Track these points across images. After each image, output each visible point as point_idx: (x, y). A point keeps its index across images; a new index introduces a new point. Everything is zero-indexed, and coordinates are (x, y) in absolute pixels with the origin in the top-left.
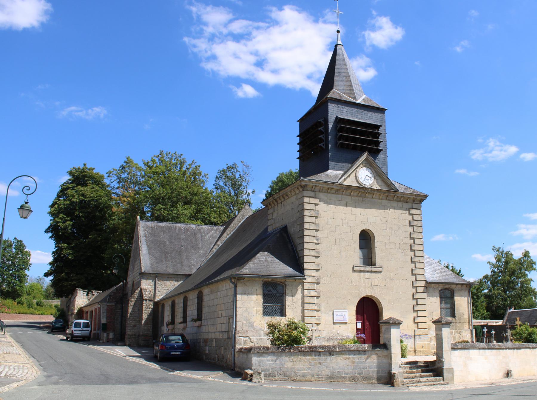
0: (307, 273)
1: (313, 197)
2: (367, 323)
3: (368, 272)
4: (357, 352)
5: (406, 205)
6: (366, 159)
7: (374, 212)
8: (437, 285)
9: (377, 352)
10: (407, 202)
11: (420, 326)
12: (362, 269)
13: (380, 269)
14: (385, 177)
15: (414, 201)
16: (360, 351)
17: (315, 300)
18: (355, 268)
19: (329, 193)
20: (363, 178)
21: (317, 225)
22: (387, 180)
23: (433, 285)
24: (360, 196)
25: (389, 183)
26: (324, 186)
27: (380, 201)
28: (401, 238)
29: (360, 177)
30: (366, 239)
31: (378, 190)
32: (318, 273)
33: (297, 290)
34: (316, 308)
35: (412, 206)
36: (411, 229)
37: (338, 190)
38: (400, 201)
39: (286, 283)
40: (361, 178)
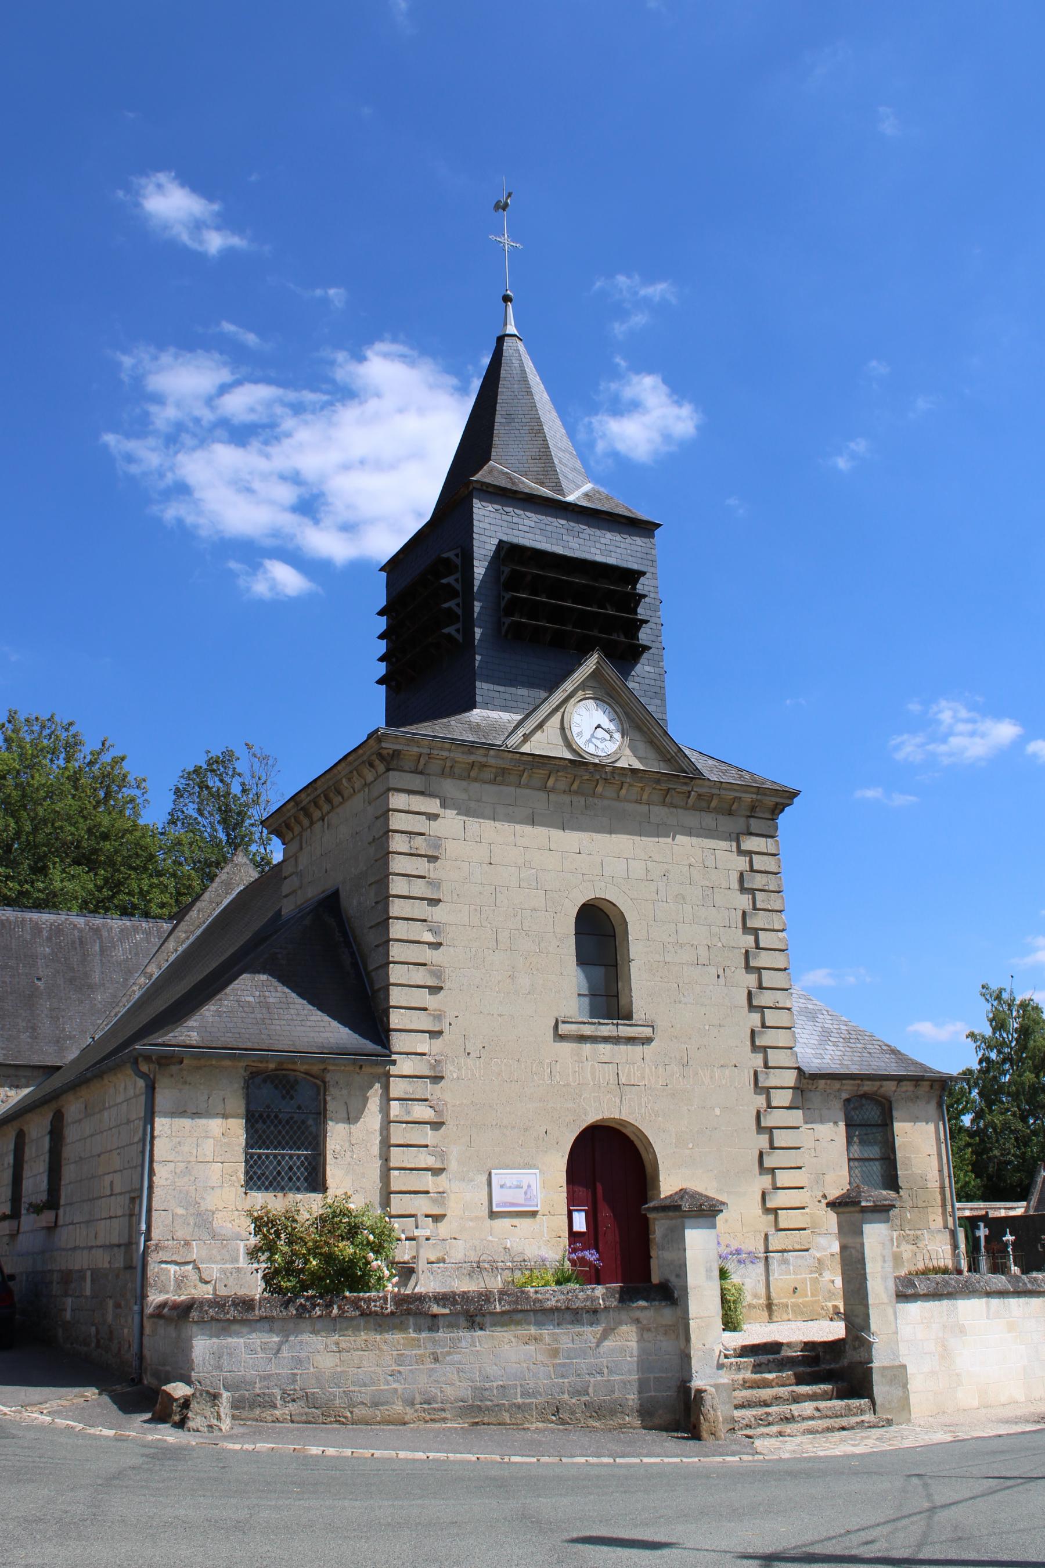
0: (399, 1042)
1: (422, 793)
2: (605, 1213)
3: (606, 1040)
4: (568, 1316)
5: (726, 823)
6: (595, 675)
7: (622, 843)
8: (837, 1085)
9: (638, 1314)
10: (730, 813)
11: (786, 1219)
12: (587, 1030)
13: (647, 1032)
14: (657, 732)
15: (752, 812)
16: (576, 1312)
17: (429, 1136)
18: (563, 1029)
19: (476, 780)
20: (587, 735)
21: (435, 884)
22: (665, 742)
23: (822, 1083)
24: (576, 793)
25: (673, 750)
26: (459, 756)
27: (644, 808)
28: (714, 929)
29: (575, 730)
30: (599, 933)
31: (634, 771)
32: (438, 1042)
33: (366, 1100)
34: (431, 1161)
35: (748, 826)
36: (744, 901)
37: (503, 771)
38: (708, 810)
39: (328, 1077)
40: (580, 734)
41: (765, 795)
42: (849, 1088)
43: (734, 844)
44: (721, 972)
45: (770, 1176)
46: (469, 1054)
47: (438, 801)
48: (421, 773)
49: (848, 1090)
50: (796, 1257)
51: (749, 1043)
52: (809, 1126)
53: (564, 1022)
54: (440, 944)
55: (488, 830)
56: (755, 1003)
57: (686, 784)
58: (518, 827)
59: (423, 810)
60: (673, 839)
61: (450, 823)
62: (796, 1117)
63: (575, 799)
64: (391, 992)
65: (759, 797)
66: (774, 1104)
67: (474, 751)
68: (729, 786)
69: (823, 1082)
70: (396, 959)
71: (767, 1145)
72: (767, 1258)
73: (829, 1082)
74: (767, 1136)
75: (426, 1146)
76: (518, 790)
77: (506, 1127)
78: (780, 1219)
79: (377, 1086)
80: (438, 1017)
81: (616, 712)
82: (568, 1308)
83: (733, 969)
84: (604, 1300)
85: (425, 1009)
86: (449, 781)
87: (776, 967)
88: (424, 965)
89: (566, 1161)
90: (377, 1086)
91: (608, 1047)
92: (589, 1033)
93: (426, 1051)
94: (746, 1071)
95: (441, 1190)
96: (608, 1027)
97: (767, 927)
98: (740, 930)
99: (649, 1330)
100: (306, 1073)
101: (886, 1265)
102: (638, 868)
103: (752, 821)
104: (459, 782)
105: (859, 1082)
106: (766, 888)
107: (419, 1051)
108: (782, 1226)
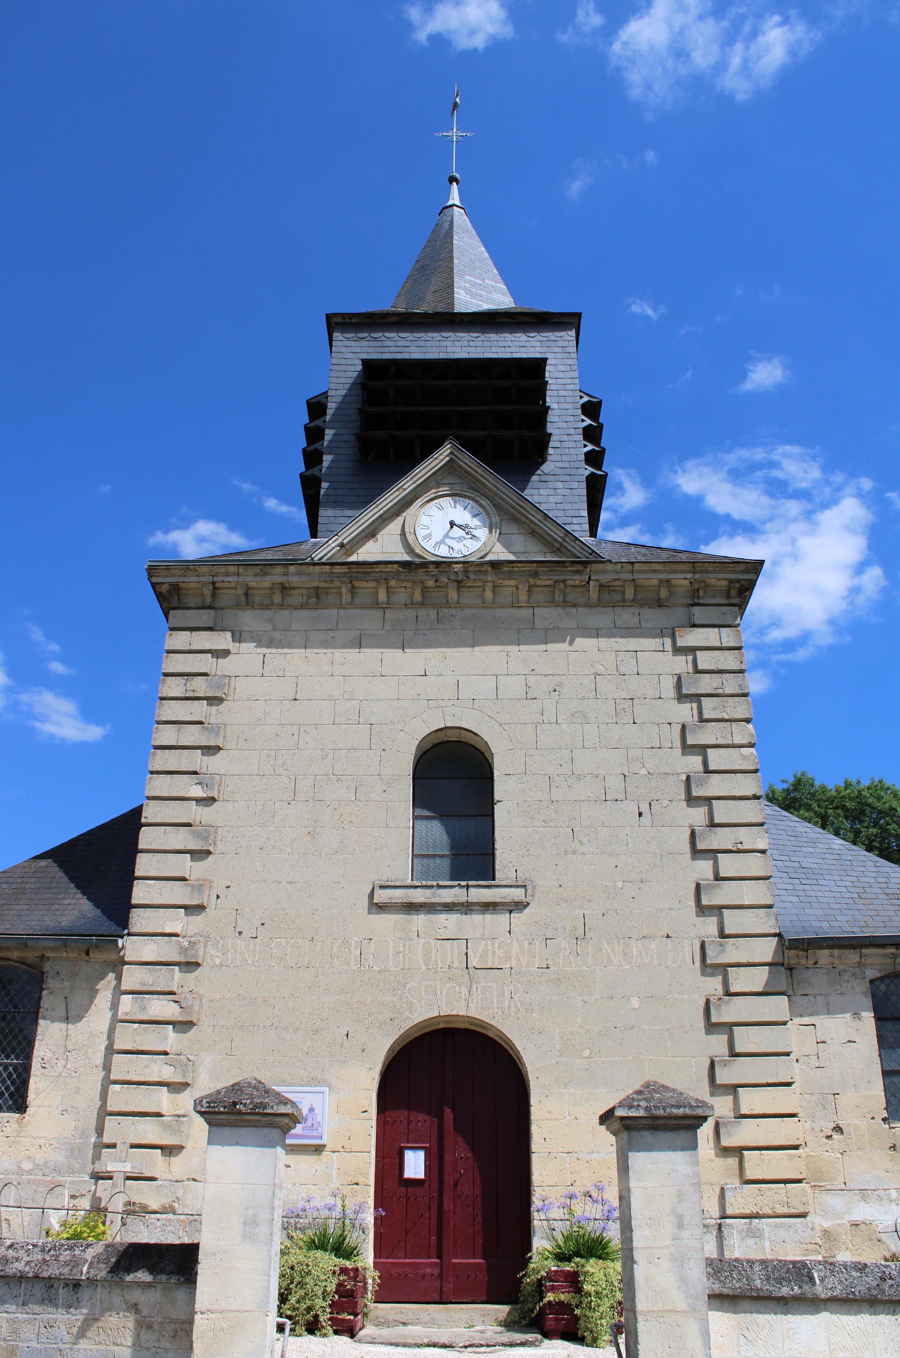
0: (139, 920)
1: (211, 629)
2: (459, 1151)
3: (450, 907)
4: (38, 1290)
5: (653, 617)
6: (450, 467)
7: (492, 656)
8: (852, 957)
9: (137, 1296)
10: (659, 604)
11: (757, 1165)
12: (419, 896)
13: (517, 894)
14: (535, 517)
15: (695, 597)
16: (50, 1283)
17: (170, 1039)
18: (381, 896)
19: (282, 606)
20: (437, 536)
21: (216, 729)
22: (548, 528)
23: (824, 955)
24: (422, 604)
25: (558, 535)
26: (252, 580)
27: (527, 613)
28: (633, 753)
29: (421, 533)
31: (496, 565)
32: (196, 923)
33: (94, 993)
34: (168, 1073)
35: (690, 617)
36: (686, 712)
37: (317, 592)
38: (622, 603)
39: (47, 967)
40: (428, 537)
41: (707, 572)
42: (878, 961)
43: (668, 641)
44: (644, 808)
45: (730, 1098)
46: (240, 933)
47: (228, 635)
48: (210, 607)
49: (876, 963)
50: (776, 1226)
51: (692, 903)
52: (806, 1020)
53: (382, 887)
54: (213, 800)
55: (298, 662)
56: (700, 846)
57: (578, 572)
58: (338, 653)
59: (207, 647)
60: (571, 644)
61: (246, 657)
62: (778, 1006)
63: (422, 613)
64: (138, 860)
65: (697, 576)
66: (733, 989)
67: (268, 570)
68: (646, 567)
69: (825, 953)
70: (149, 821)
71: (725, 1051)
72: (720, 1225)
73: (836, 952)
74: (725, 1037)
75: (166, 1053)
76: (342, 612)
77: (285, 1028)
78: (747, 1165)
79: (111, 976)
80: (199, 888)
81: (481, 506)
82: (36, 1277)
83: (665, 803)
84: (90, 1267)
85: (184, 879)
86: (248, 612)
87: (738, 794)
88: (189, 825)
89: (377, 1078)
90: (111, 976)
91: (453, 918)
92: (421, 900)
93: (178, 931)
94: (687, 944)
95: (181, 1112)
96: (453, 890)
97: (720, 741)
98: (678, 751)
99: (150, 1327)
100: (21, 963)
101: (685, 1234)
102: (513, 686)
103: (696, 610)
104: (261, 612)
105: (893, 950)
106: (721, 691)
107: (167, 931)
108: (750, 1174)
